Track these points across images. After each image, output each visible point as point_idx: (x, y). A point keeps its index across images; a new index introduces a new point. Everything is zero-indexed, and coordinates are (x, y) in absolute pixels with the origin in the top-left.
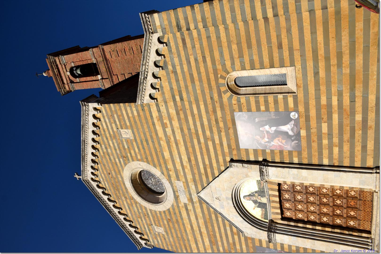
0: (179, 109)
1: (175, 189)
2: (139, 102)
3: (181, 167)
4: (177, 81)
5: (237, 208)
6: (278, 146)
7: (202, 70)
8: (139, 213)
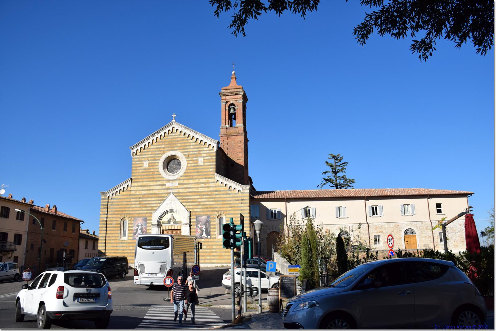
0: (212, 192)
2: (216, 174)
4: (224, 194)
7: (227, 206)
8: (155, 154)
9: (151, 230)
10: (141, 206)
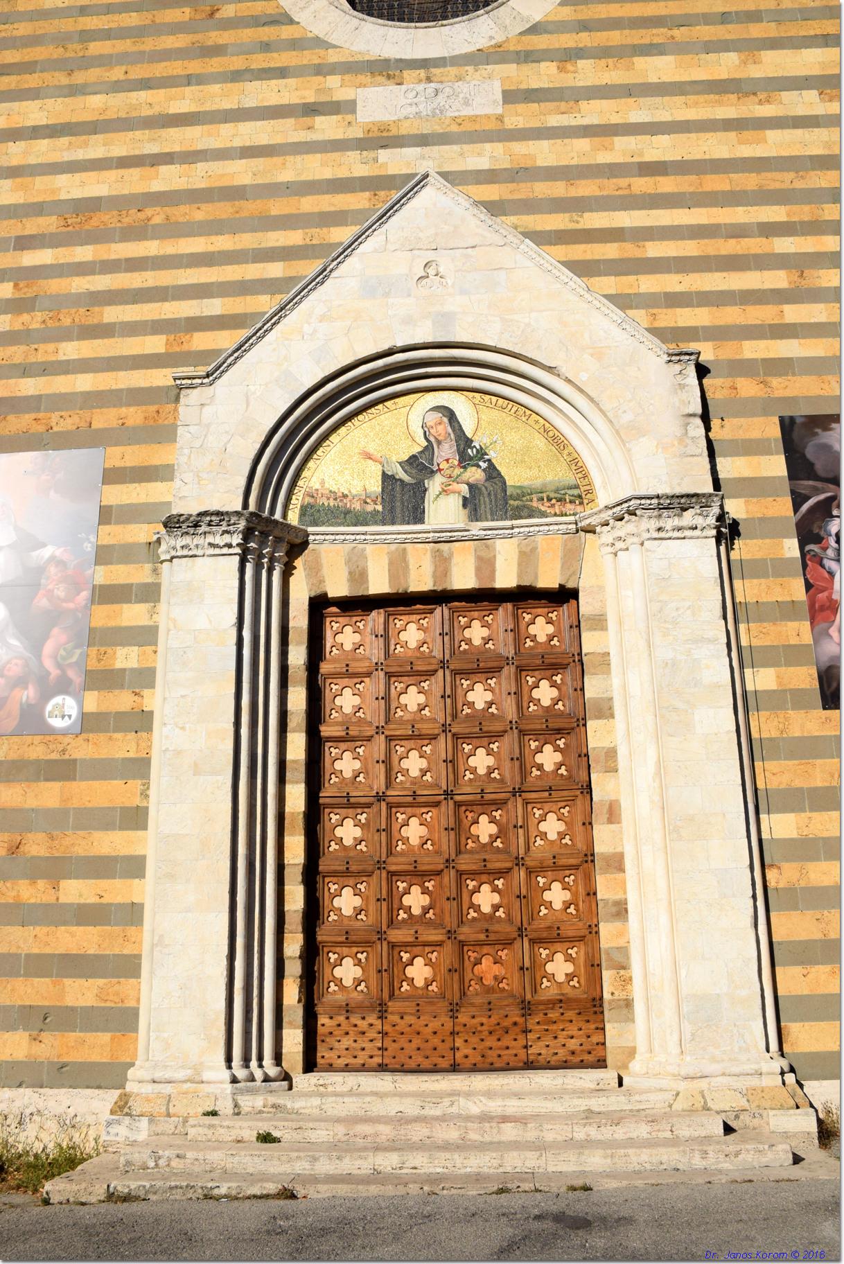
1: (442, 70)
3: (596, 122)
5: (380, 363)
6: (830, 599)
9: (150, 593)
10: (34, 321)
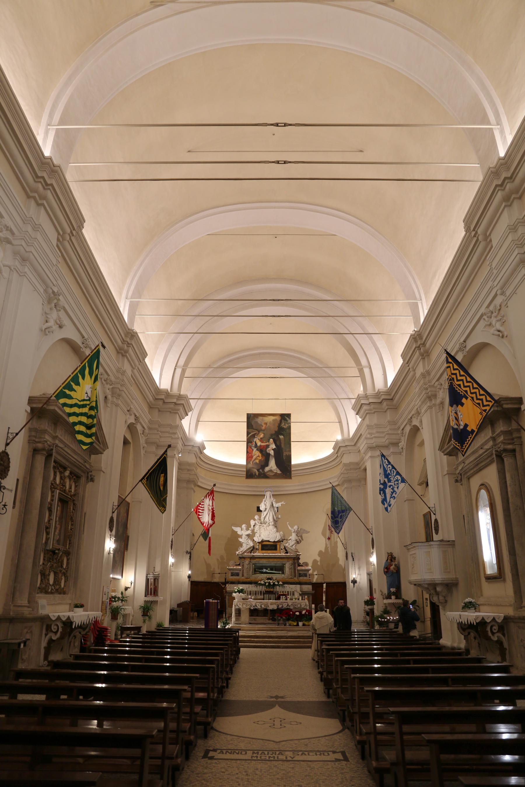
6: (252, 455)
